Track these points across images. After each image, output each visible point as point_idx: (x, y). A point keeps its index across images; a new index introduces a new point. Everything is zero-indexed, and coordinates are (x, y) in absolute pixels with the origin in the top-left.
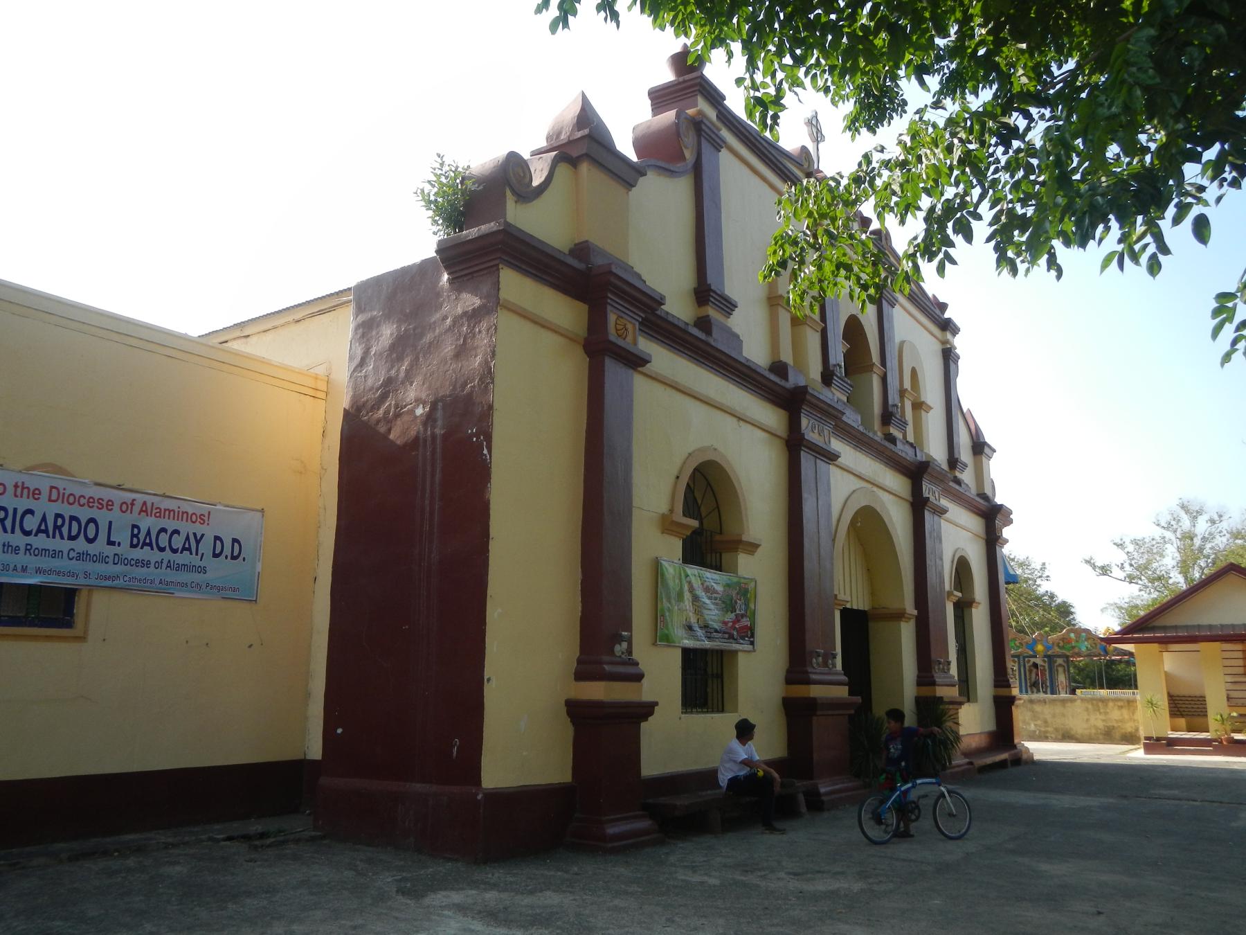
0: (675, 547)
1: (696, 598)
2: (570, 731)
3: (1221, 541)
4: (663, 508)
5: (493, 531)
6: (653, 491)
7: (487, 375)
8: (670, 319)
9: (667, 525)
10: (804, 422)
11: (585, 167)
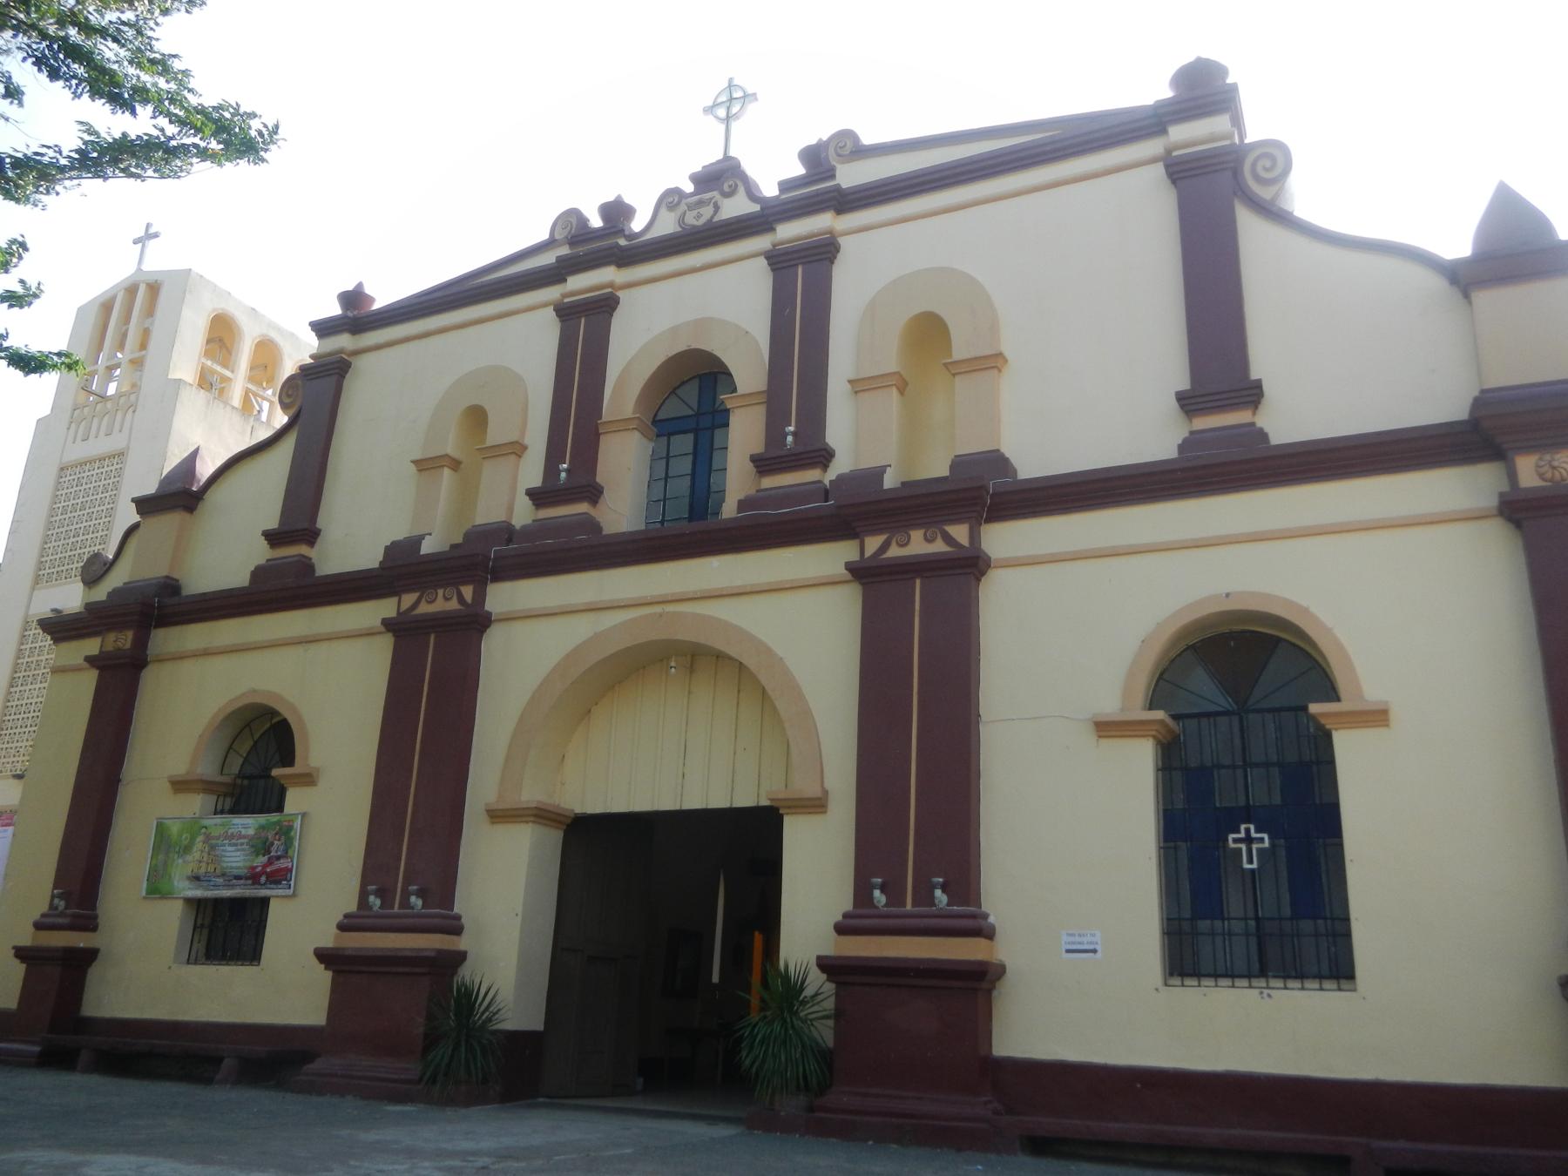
0: (195, 804)
1: (213, 847)
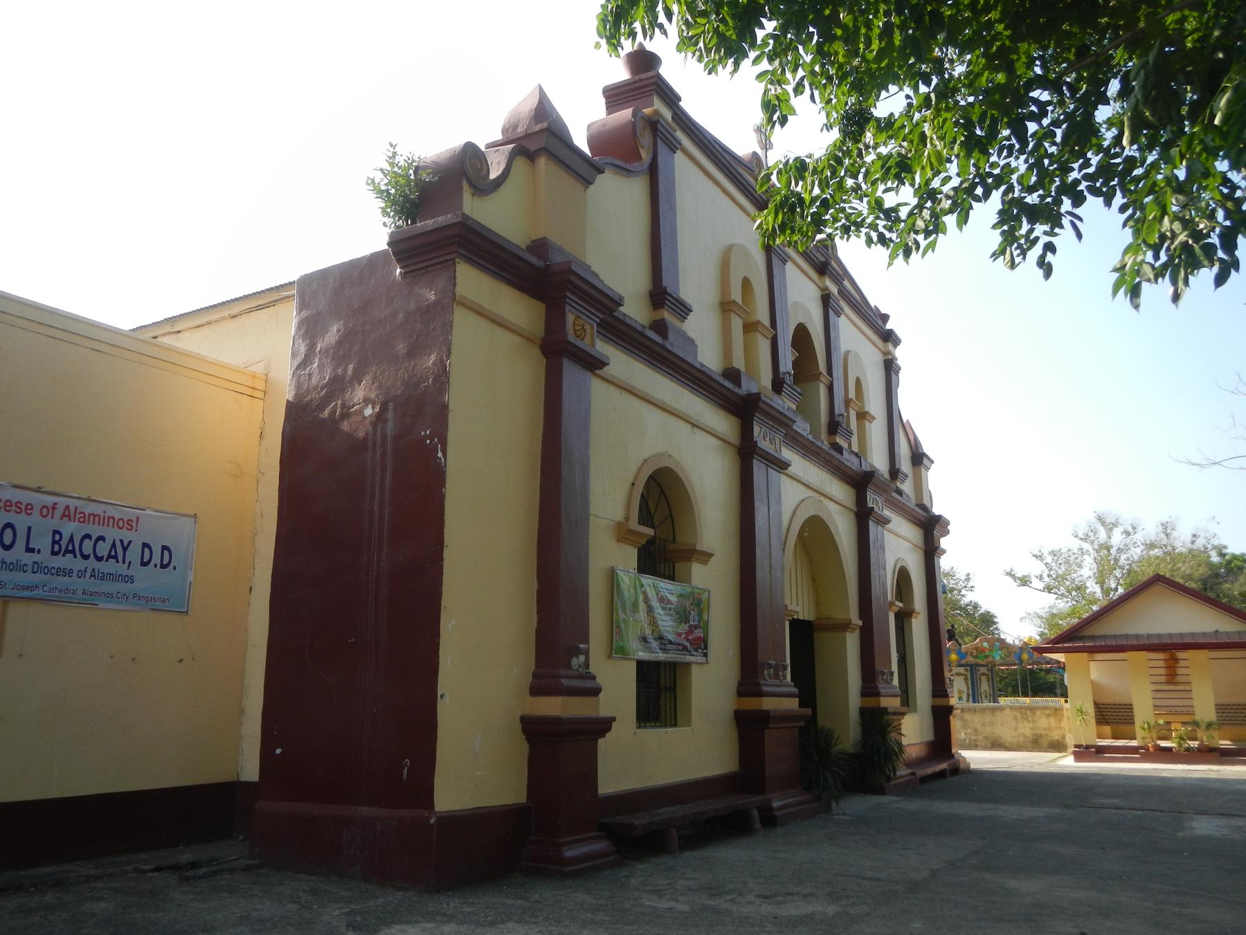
2: (525, 748)
3: (1136, 553)
4: (617, 514)
5: (446, 542)
6: (609, 498)
7: (442, 376)
8: (628, 321)
9: (623, 534)
10: (756, 429)
11: (542, 162)
